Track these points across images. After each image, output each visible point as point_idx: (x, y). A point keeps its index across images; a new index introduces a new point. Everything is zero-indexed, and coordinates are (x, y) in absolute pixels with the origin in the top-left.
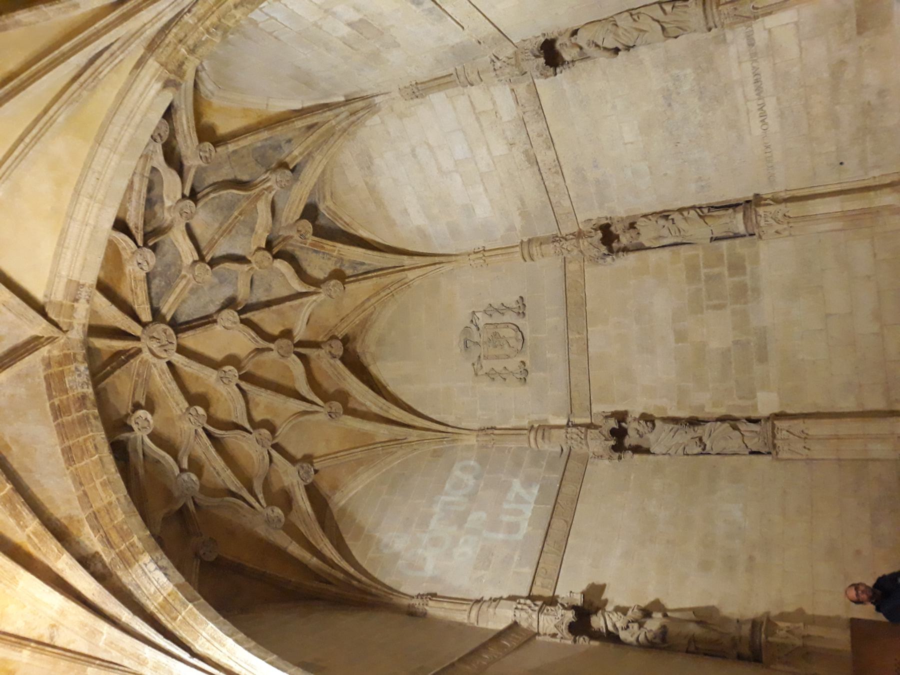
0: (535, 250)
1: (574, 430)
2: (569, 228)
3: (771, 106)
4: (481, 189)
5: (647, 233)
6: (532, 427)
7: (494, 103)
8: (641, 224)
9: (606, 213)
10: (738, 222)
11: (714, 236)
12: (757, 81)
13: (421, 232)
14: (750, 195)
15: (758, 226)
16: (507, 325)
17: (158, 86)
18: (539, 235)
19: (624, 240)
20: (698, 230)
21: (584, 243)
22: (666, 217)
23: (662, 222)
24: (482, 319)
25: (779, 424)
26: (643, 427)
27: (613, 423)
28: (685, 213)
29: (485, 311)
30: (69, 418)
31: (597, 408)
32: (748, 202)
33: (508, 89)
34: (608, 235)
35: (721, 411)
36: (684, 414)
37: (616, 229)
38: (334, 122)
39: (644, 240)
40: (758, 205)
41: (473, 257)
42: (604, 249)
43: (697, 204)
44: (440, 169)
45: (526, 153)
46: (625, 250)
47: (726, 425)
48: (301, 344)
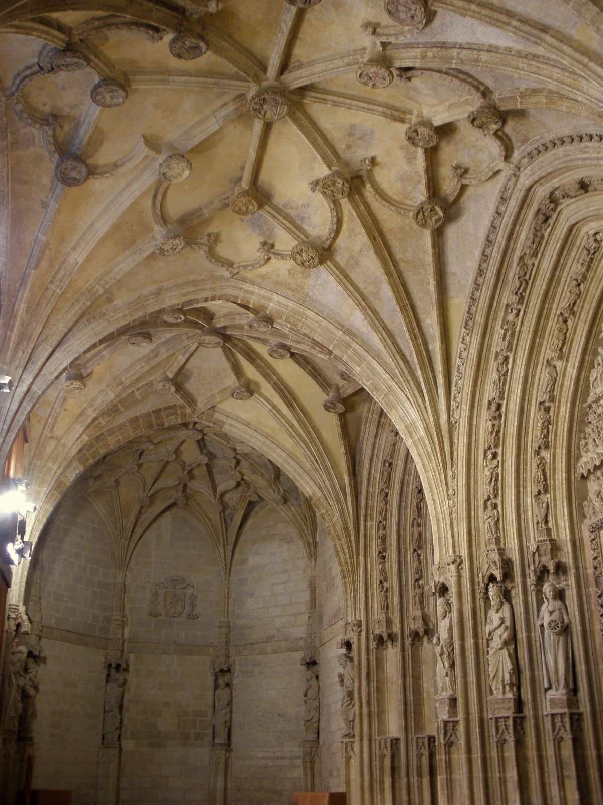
0: (224, 630)
1: (121, 643)
2: (232, 650)
3: (271, 763)
4: (261, 605)
5: (223, 693)
6: (123, 617)
7: (299, 626)
8: (227, 691)
9: (236, 672)
10: (220, 739)
11: (216, 728)
12: (281, 758)
13: (244, 561)
14: (233, 747)
15: (216, 750)
16: (183, 607)
17: (310, 493)
18: (232, 633)
19: (221, 682)
21: (222, 659)
22: (228, 704)
23: (226, 702)
24: (189, 591)
25: (117, 750)
26: (121, 681)
27: (123, 666)
28: (229, 714)
29: (193, 594)
30: (153, 419)
31: (132, 657)
32: (229, 745)
33: (304, 636)
35: (125, 722)
36: (125, 703)
37: (227, 676)
38: (306, 532)
39: (218, 691)
40: (226, 750)
41: (226, 591)
42: (217, 670)
43: (233, 720)
45: (273, 637)
46: (216, 679)
47: (118, 724)
48: (185, 486)
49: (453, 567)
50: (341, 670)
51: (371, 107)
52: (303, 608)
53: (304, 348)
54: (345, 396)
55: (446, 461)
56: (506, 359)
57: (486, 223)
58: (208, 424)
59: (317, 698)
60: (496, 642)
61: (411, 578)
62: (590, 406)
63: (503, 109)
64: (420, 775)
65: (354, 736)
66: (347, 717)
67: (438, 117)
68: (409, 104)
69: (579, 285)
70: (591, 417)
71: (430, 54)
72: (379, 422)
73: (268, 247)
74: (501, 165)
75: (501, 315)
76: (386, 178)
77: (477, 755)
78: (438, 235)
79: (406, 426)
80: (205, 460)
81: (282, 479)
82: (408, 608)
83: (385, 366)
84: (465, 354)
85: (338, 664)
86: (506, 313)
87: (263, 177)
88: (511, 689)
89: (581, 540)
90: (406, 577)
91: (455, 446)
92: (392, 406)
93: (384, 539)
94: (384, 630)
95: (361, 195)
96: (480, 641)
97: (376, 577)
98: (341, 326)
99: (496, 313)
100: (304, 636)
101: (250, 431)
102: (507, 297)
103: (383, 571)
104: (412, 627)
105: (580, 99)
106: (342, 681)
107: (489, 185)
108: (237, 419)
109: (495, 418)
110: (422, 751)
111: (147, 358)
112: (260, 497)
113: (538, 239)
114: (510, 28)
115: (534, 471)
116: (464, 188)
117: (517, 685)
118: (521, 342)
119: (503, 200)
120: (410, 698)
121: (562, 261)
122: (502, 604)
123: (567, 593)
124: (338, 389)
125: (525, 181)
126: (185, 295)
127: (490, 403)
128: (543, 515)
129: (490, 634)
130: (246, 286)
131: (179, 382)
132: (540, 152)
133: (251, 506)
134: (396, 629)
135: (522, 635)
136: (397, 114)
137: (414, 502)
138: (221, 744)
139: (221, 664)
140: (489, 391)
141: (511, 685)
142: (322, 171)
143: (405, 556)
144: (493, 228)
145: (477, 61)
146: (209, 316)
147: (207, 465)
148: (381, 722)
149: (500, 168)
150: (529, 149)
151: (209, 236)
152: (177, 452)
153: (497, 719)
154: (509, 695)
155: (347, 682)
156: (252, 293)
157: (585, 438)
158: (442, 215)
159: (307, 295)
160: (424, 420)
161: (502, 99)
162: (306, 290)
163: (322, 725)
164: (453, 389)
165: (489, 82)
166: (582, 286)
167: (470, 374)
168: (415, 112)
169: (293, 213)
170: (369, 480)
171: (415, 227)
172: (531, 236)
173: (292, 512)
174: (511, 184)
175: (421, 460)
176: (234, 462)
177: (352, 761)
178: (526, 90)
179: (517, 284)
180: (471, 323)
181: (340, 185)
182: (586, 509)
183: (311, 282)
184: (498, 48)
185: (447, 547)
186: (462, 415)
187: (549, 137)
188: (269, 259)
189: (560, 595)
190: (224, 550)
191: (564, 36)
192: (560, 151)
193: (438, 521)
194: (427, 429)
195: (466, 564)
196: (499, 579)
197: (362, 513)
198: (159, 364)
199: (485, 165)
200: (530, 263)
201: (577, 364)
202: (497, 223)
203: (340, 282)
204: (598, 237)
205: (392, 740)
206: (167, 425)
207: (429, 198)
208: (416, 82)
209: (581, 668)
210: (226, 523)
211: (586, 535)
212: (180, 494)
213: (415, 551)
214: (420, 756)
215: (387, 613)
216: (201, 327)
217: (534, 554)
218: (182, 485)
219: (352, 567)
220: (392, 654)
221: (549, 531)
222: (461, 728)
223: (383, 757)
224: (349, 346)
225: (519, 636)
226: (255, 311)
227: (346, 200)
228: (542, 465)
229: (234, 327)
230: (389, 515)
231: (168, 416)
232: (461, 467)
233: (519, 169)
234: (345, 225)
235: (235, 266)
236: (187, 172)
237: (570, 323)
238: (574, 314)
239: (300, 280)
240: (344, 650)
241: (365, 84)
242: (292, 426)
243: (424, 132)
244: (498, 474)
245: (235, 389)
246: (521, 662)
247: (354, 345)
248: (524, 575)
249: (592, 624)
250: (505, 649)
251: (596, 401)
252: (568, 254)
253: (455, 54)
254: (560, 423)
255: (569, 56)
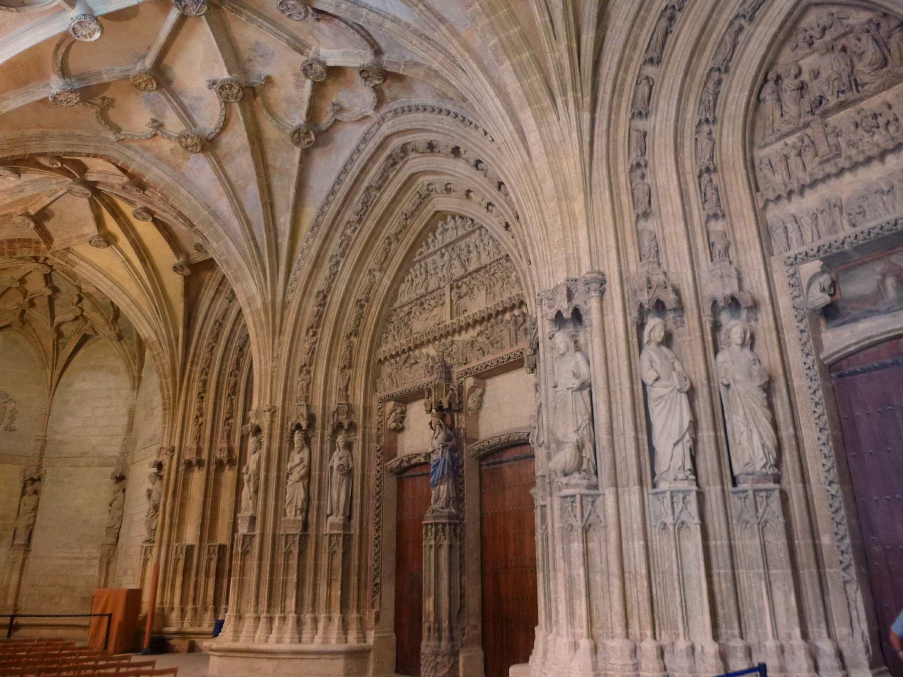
0: (40, 443)
2: (45, 461)
3: (67, 562)
8: (35, 497)
10: (20, 541)
13: (68, 385)
14: (33, 547)
17: (147, 336)
19: (29, 489)
20: (22, 523)
21: (34, 469)
22: (34, 509)
33: (117, 454)
34: (35, 480)
37: (37, 484)
39: (25, 498)
40: (25, 551)
42: (28, 478)
44: (96, 408)
45: (88, 453)
46: (25, 487)
48: (23, 312)
49: (267, 414)
50: (150, 486)
51: (279, 32)
52: (121, 430)
53: (168, 217)
54: (193, 262)
55: (277, 331)
56: (338, 263)
57: (346, 153)
58: (60, 261)
59: (122, 508)
60: (295, 476)
61: (223, 416)
62: (395, 310)
63: (388, 69)
64: (207, 576)
65: (154, 542)
66: (150, 526)
67: (332, 59)
68: (310, 40)
69: (407, 219)
70: (394, 319)
71: (343, 6)
72: (217, 290)
73: (158, 125)
74: (371, 112)
75: (341, 228)
76: (276, 95)
77: (267, 562)
78: (306, 155)
79: (248, 299)
80: (49, 292)
81: (119, 320)
82: (216, 441)
83: (239, 246)
84: (306, 252)
85: (147, 480)
86: (345, 227)
87: (166, 61)
88: (301, 513)
89: (371, 407)
90: (219, 414)
91: (285, 321)
92: (237, 280)
93: (205, 383)
94: (194, 456)
95: (251, 105)
96: (282, 474)
97: (193, 412)
98: (208, 207)
99: (338, 225)
100: (117, 454)
101: (101, 276)
102: (349, 215)
103: (200, 409)
104: (218, 456)
105: (454, 83)
106: (149, 496)
107: (356, 127)
108: (89, 263)
109: (320, 305)
110: (213, 556)
111: (11, 192)
112: (95, 332)
113: (384, 178)
114: (416, 9)
115: (343, 350)
116: (336, 122)
117: (306, 510)
118: (352, 252)
119: (365, 140)
120: (208, 513)
121: (398, 198)
122: (303, 448)
123: (355, 446)
124: (188, 256)
125: (385, 129)
126: (68, 145)
127: (319, 293)
128: (345, 384)
129: (291, 469)
130: (130, 153)
131: (41, 218)
132: (404, 111)
133: (85, 339)
134: (205, 456)
135: (315, 473)
136: (298, 44)
137: (235, 357)
138: (20, 545)
139: (32, 472)
140: (320, 284)
141: (302, 510)
142: (222, 74)
143: (221, 399)
144: (351, 160)
145: (381, 25)
146: (83, 169)
147: (49, 297)
148: (180, 531)
149: (369, 114)
150: (396, 107)
151: (103, 99)
152: (22, 281)
153: (287, 536)
154: (300, 518)
155: (154, 496)
156: (134, 160)
157: (387, 333)
158: (313, 138)
159: (183, 174)
160: (263, 296)
161: (389, 62)
162: (183, 170)
163: (122, 531)
164: (292, 276)
165: (383, 44)
166: (408, 222)
167: (307, 267)
168: (313, 48)
169: (186, 102)
170: (200, 334)
171: (289, 142)
172: (379, 174)
173: (124, 350)
174: (373, 129)
175: (255, 326)
176: (76, 299)
177: (149, 563)
178: (410, 61)
179: (360, 207)
180: (316, 229)
181: (235, 91)
182: (378, 385)
183: (189, 164)
184: (400, 20)
185: (265, 398)
186: (294, 298)
187: (415, 101)
188: (156, 135)
189: (349, 446)
190: (52, 373)
191: (455, 31)
192: (420, 115)
193: (261, 376)
194: (264, 303)
195: (279, 414)
196: (304, 428)
197: (190, 359)
198: (22, 200)
199: (357, 109)
200: (373, 193)
201: (392, 277)
202: (355, 157)
203: (216, 171)
204: (430, 187)
205: (187, 547)
206: (19, 255)
207: (306, 122)
208: (322, 25)
209: (357, 502)
210: (57, 349)
211: (375, 404)
212: (17, 318)
213: (229, 396)
214: (209, 560)
215: (198, 443)
216: (73, 177)
217: (334, 413)
218: (20, 310)
219: (174, 402)
220: (198, 477)
221: (347, 396)
222: (257, 540)
223: (177, 561)
224: (211, 225)
225: (313, 473)
226: (131, 176)
227: (236, 104)
228: (350, 347)
229: (105, 184)
230: (212, 364)
231: (21, 247)
232: (287, 338)
233: (383, 119)
234: (230, 125)
235: (122, 132)
236: (97, 35)
237: (393, 246)
238: (398, 240)
239: (180, 161)
240: (155, 470)
241: (283, 12)
242: (140, 278)
243: (319, 68)
244: (314, 348)
245: (94, 237)
246: (311, 494)
247: (216, 225)
248: (323, 428)
249: (369, 471)
250: (301, 484)
251: (401, 307)
252: (404, 194)
253: (364, 13)
254: (369, 318)
255: (456, 48)
